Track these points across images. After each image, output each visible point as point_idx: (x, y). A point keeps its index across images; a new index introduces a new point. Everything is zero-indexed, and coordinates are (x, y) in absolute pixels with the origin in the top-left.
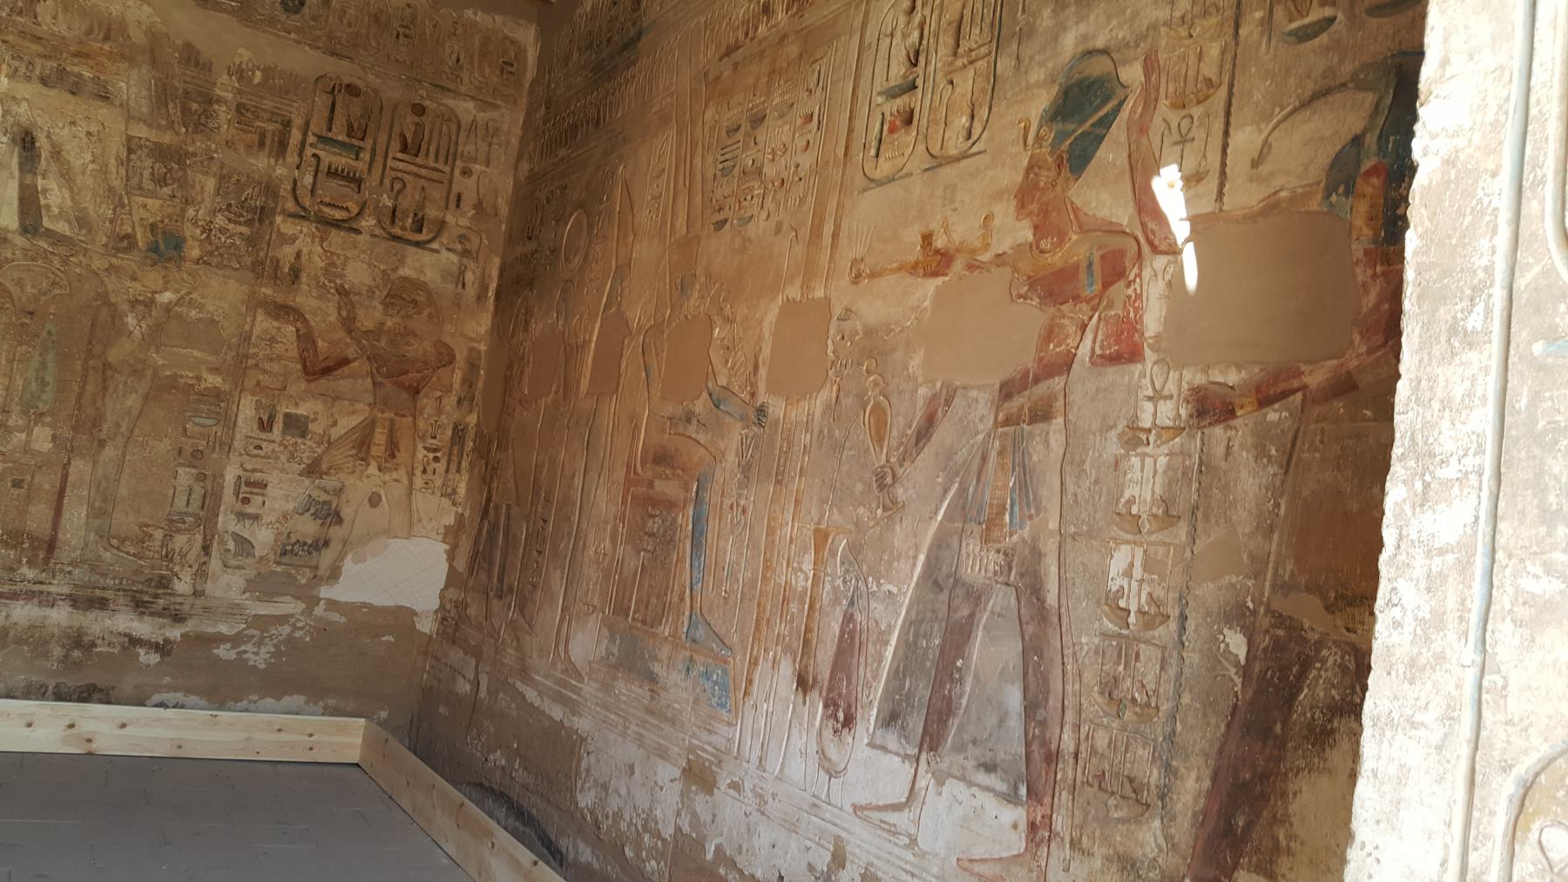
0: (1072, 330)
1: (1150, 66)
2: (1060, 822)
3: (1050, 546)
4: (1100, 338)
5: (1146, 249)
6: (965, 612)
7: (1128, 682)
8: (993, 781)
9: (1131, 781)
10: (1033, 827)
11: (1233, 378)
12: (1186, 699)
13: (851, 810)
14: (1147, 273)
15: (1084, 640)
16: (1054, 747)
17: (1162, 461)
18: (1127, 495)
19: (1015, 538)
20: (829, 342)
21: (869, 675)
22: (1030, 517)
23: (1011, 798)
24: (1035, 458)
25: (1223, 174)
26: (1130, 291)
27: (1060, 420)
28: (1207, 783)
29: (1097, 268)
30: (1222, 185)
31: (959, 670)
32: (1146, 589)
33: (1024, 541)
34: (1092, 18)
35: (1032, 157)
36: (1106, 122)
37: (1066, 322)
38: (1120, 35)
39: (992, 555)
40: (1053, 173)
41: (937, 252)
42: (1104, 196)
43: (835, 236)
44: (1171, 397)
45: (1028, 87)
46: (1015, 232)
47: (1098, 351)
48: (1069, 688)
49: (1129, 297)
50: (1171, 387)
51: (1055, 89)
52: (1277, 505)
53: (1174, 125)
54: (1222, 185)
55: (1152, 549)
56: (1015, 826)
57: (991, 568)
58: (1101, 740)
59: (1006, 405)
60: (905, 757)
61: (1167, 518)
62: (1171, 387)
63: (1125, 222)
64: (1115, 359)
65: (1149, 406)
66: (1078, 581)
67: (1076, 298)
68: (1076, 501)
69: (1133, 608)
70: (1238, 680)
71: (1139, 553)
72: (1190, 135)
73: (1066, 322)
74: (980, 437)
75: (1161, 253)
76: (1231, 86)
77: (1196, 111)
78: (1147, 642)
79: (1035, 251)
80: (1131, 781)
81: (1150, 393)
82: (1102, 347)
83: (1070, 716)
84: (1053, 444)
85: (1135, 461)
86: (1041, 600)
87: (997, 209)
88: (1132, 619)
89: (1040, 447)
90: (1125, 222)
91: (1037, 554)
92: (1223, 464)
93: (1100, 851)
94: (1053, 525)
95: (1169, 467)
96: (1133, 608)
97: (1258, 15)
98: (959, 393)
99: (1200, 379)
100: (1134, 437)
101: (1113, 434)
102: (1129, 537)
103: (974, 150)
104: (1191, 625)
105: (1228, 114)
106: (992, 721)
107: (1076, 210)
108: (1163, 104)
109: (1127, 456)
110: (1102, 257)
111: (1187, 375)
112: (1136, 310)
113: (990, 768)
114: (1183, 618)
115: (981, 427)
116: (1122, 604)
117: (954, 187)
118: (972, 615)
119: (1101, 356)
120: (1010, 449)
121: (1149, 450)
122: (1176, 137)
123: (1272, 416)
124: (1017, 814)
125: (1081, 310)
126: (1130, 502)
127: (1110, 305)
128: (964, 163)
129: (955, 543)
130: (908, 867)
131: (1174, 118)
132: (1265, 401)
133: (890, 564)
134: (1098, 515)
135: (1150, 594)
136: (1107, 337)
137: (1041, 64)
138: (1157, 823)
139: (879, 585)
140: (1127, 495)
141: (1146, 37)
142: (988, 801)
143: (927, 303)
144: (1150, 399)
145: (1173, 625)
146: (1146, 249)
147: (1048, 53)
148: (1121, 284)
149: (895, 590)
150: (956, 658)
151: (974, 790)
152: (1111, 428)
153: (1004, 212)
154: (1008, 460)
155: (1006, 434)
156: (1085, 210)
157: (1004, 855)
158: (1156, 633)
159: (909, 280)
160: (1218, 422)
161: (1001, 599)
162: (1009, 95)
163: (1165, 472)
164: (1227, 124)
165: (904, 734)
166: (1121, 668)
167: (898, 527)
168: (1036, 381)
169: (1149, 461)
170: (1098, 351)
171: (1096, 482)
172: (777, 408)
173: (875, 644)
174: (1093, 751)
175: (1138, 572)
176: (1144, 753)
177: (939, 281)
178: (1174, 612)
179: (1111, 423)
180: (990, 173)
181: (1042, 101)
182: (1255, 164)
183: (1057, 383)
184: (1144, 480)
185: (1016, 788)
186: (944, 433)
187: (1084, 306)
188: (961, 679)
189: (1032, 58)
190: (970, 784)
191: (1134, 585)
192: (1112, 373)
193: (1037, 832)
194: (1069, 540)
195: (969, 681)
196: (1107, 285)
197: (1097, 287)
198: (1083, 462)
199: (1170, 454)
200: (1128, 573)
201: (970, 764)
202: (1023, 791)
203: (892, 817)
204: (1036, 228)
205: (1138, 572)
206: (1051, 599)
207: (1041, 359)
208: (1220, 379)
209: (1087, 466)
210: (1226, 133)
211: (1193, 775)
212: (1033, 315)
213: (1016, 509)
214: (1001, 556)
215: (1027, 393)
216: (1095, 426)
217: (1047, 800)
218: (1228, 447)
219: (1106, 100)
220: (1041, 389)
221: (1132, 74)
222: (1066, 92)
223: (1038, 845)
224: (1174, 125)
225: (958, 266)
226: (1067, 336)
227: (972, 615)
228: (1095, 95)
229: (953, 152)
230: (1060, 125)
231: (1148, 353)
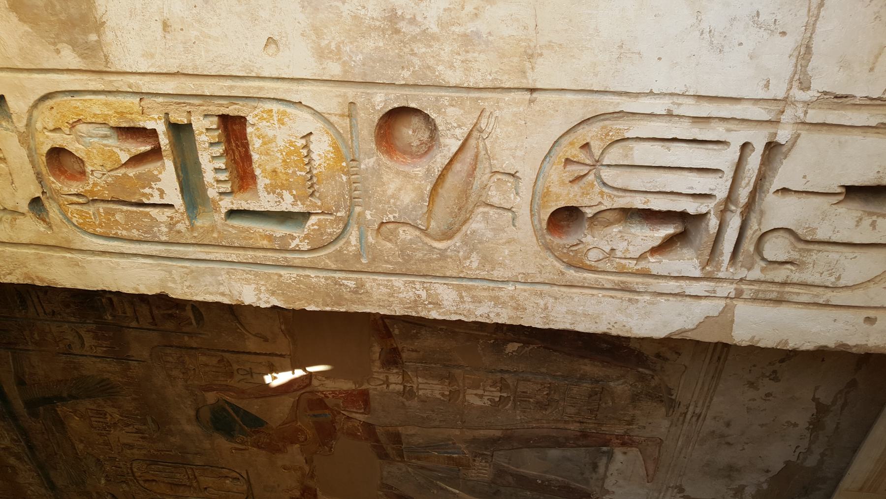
0: (350, 424)
1: (208, 388)
2: (619, 431)
3: (469, 434)
5: (308, 389)
6: (510, 479)
9: (590, 396)
10: (623, 444)
11: (377, 349)
12: (543, 370)
14: (321, 389)
16: (578, 434)
17: (420, 380)
18: (439, 396)
22: (454, 444)
23: (610, 455)
24: (421, 441)
25: (270, 354)
26: (330, 396)
27: (400, 428)
28: (586, 361)
30: (277, 355)
32: (488, 388)
33: (467, 447)
36: (236, 409)
37: (346, 426)
39: (477, 464)
41: (302, 495)
46: (294, 454)
47: (362, 411)
48: (545, 425)
50: (382, 377)
51: (216, 434)
52: (441, 329)
53: (242, 377)
54: (277, 355)
56: (625, 453)
57: (484, 464)
58: (571, 410)
61: (451, 378)
62: (382, 377)
63: (292, 400)
65: (392, 387)
67: (333, 422)
68: (444, 421)
69: (499, 394)
70: (531, 347)
71: (469, 391)
73: (346, 426)
74: (410, 469)
75: (310, 382)
76: (223, 351)
77: (235, 367)
78: (516, 388)
80: (590, 396)
83: (561, 425)
84: (413, 432)
85: (421, 392)
86: (499, 439)
88: (505, 395)
91: (474, 440)
92: (421, 353)
94: (457, 432)
95: (424, 377)
96: (499, 394)
97: (186, 338)
99: (378, 363)
100: (409, 393)
101: (407, 403)
102: (461, 395)
103: (245, 476)
104: (505, 368)
105: (238, 352)
107: (284, 423)
108: (230, 382)
109: (419, 397)
110: (311, 410)
111: (375, 369)
114: (502, 371)
115: (404, 470)
116: (497, 399)
118: (512, 475)
121: (415, 386)
123: (397, 332)
126: (443, 395)
127: (338, 405)
128: (252, 481)
131: (238, 377)
132: (389, 335)
138: (612, 384)
140: (439, 396)
144: (388, 386)
145: (506, 376)
146: (308, 389)
148: (326, 401)
158: (511, 384)
160: (400, 355)
164: (244, 353)
166: (531, 400)
168: (378, 441)
169: (420, 386)
170: (362, 411)
171: (433, 411)
174: (578, 414)
175: (480, 392)
176: (575, 390)
177: (319, 493)
178: (499, 375)
181: (223, 443)
182: (266, 340)
183: (379, 431)
184: (432, 389)
185: (604, 452)
188: (548, 481)
191: (486, 393)
193: (626, 442)
195: (548, 476)
196: (326, 407)
197: (327, 412)
200: (481, 397)
201: (594, 476)
202: (605, 449)
204: (292, 443)
205: (480, 392)
206: (498, 433)
208: (378, 355)
209: (425, 415)
210: (249, 353)
211: (583, 367)
213: (450, 451)
215: (385, 446)
217: (608, 437)
218: (413, 351)
219: (224, 409)
220: (383, 439)
221: (211, 397)
222: (217, 429)
223: (634, 442)
224: (242, 377)
225: (310, 483)
226: (354, 426)
227: (512, 475)
229: (245, 487)
231: (363, 387)
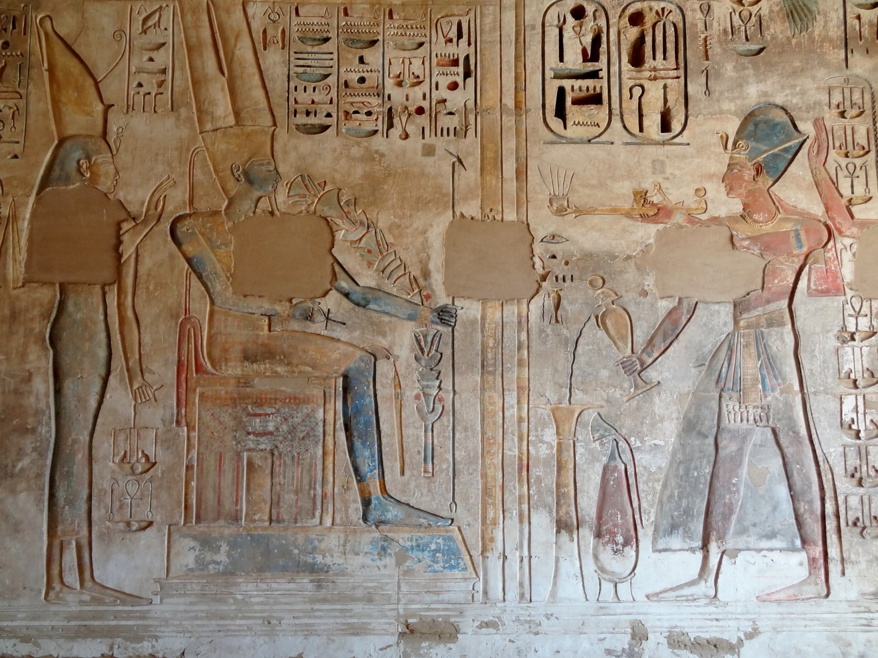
1: (818, 123)
4: (813, 279)
5: (836, 233)
7: (864, 468)
8: (776, 543)
10: (812, 561)
13: (646, 599)
14: (839, 246)
15: (832, 450)
19: (769, 398)
20: (536, 260)
21: (644, 505)
22: (779, 385)
24: (775, 349)
26: (829, 255)
27: (790, 326)
29: (803, 236)
31: (734, 485)
33: (777, 399)
34: (769, 82)
35: (731, 158)
37: (784, 267)
38: (794, 101)
40: (754, 173)
42: (800, 196)
43: (522, 173)
44: (866, 316)
45: (721, 112)
47: (813, 287)
49: (830, 258)
50: (865, 310)
53: (843, 166)
55: (868, 397)
56: (801, 564)
57: (751, 418)
58: (854, 501)
59: (745, 316)
60: (693, 550)
64: (825, 293)
66: (822, 418)
67: (790, 254)
69: (862, 428)
71: (860, 399)
72: (856, 174)
74: (724, 336)
77: (859, 162)
79: (749, 221)
81: (852, 312)
82: (815, 285)
87: (708, 186)
88: (862, 435)
89: (778, 342)
90: (820, 214)
91: (789, 406)
93: (863, 559)
95: (870, 353)
98: (699, 306)
101: (831, 335)
103: (676, 140)
106: (766, 509)
107: (780, 200)
112: (836, 268)
113: (771, 535)
117: (663, 163)
119: (816, 290)
120: (753, 343)
122: (846, 173)
124: (803, 556)
125: (793, 262)
128: (667, 147)
129: (715, 404)
130: (713, 617)
131: (844, 162)
133: (653, 425)
134: (829, 380)
135: (872, 421)
136: (819, 279)
137: (732, 100)
139: (642, 441)
140: (846, 368)
141: (814, 108)
142: (775, 555)
143: (651, 241)
144: (850, 315)
147: (736, 94)
149: (662, 443)
150: (730, 478)
151: (764, 553)
152: (828, 332)
153: (716, 191)
154: (753, 350)
155: (749, 335)
156: (787, 201)
157: (796, 582)
159: (626, 222)
161: (761, 435)
162: (705, 112)
163: (868, 355)
165: (688, 534)
167: (657, 400)
168: (768, 302)
169: (857, 350)
171: (824, 362)
172: (469, 310)
173: (646, 483)
175: (861, 409)
179: (829, 328)
180: (697, 161)
185: (793, 542)
186: (691, 333)
187: (796, 260)
189: (721, 93)
190: (760, 550)
191: (861, 416)
192: (824, 300)
194: (811, 396)
195: (742, 489)
198: (814, 350)
199: (870, 346)
202: (798, 542)
203: (686, 591)
204: (746, 206)
207: (770, 289)
212: (750, 262)
213: (767, 380)
214: (759, 410)
216: (818, 330)
219: (789, 138)
221: (806, 127)
224: (843, 166)
228: (779, 132)
230: (754, 144)
231: (847, 290)
